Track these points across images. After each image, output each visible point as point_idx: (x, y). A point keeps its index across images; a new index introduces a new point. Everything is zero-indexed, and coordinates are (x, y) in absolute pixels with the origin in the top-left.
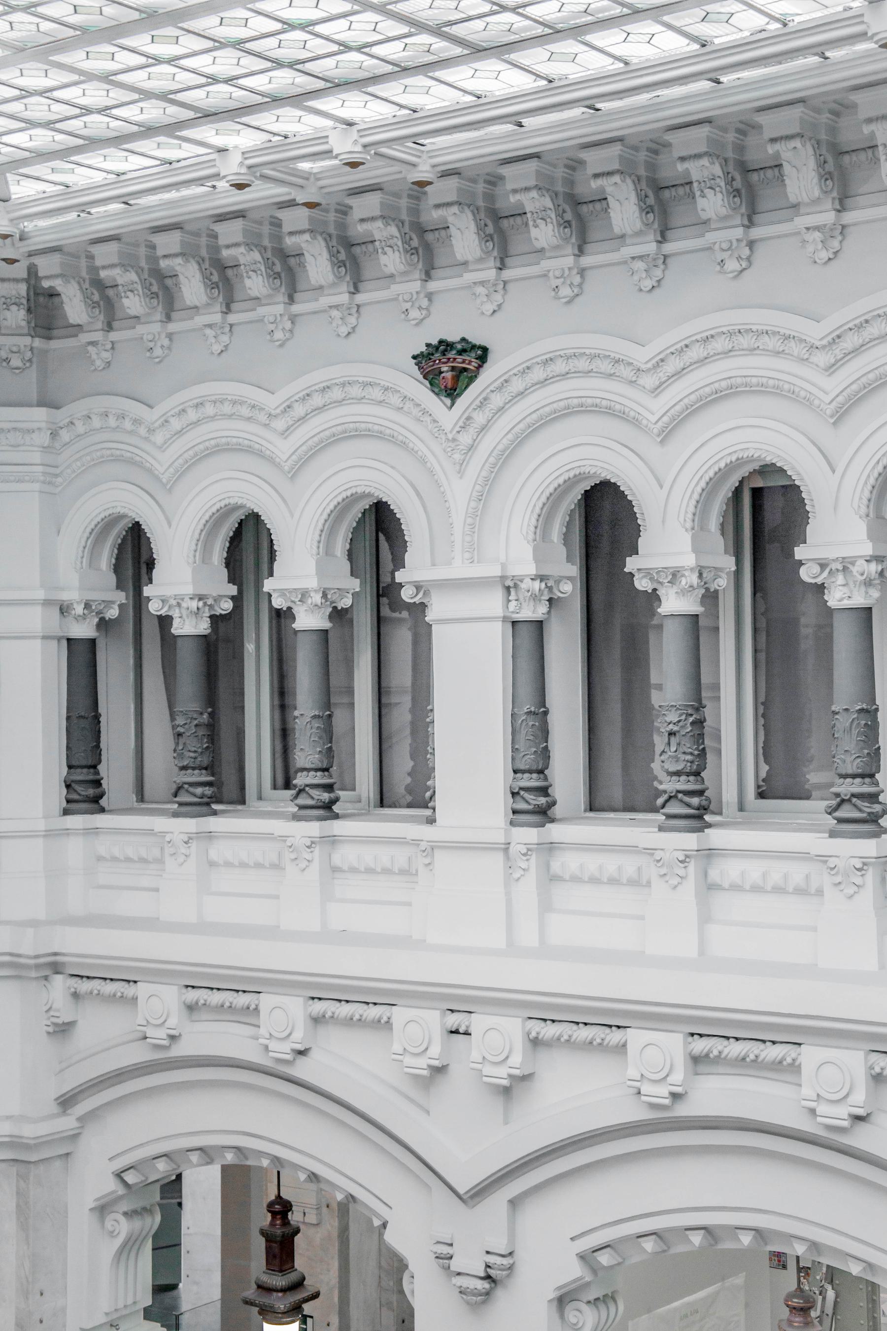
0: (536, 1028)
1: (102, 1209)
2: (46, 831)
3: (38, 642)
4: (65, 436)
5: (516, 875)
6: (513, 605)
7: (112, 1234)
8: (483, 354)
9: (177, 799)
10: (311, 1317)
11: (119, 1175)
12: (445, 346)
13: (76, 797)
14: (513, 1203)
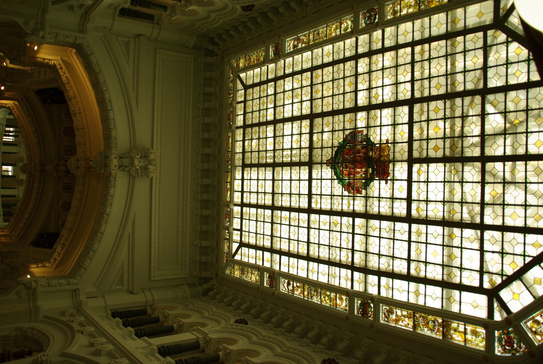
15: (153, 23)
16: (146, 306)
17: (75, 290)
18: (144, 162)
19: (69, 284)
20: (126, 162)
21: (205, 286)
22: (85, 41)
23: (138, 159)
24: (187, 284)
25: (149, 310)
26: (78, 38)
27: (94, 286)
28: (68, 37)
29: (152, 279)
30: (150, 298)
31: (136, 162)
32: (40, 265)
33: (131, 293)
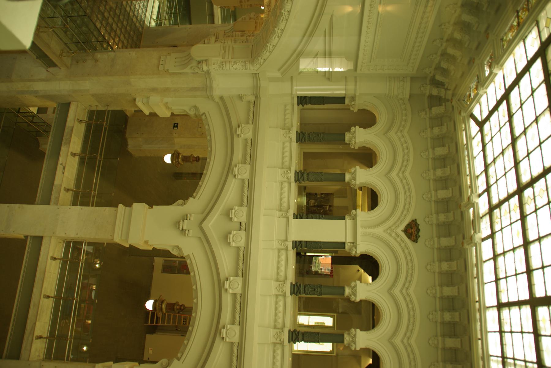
0: (242, 249)
1: (195, 107)
2: (293, 94)
4: (401, 101)
5: (280, 242)
6: (349, 244)
7: (190, 110)
9: (301, 133)
10: (177, 129)
11: (204, 114)
12: (418, 230)
13: (302, 99)
14: (200, 237)
25: (347, 101)
27: (279, 70)
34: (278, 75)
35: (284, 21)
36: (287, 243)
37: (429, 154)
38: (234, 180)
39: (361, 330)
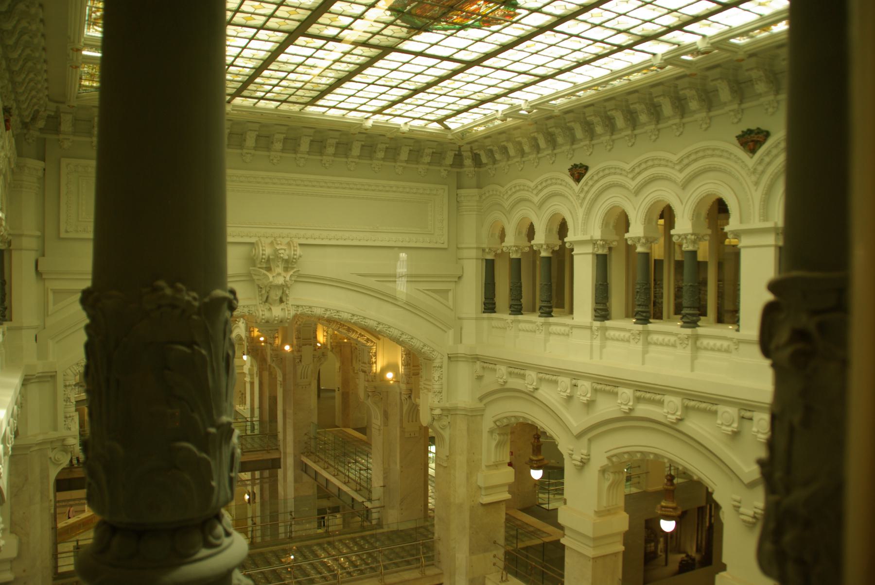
1: (491, 432)
3: (475, 260)
4: (484, 197)
6: (596, 249)
8: (586, 168)
14: (590, 440)
15: (10, 251)
16: (482, 259)
17: (449, 358)
18: (278, 266)
19: (441, 367)
20: (275, 295)
21: (468, 162)
22: (69, 370)
23: (273, 277)
24: (458, 188)
26: (68, 384)
28: (67, 400)
29: (445, 246)
30: (473, 253)
31: (280, 281)
32: (374, 360)
33: (460, 278)
34: (451, 333)
35: (366, 321)
36: (594, 328)
37: (517, 162)
38: (540, 391)
39: (727, 224)
